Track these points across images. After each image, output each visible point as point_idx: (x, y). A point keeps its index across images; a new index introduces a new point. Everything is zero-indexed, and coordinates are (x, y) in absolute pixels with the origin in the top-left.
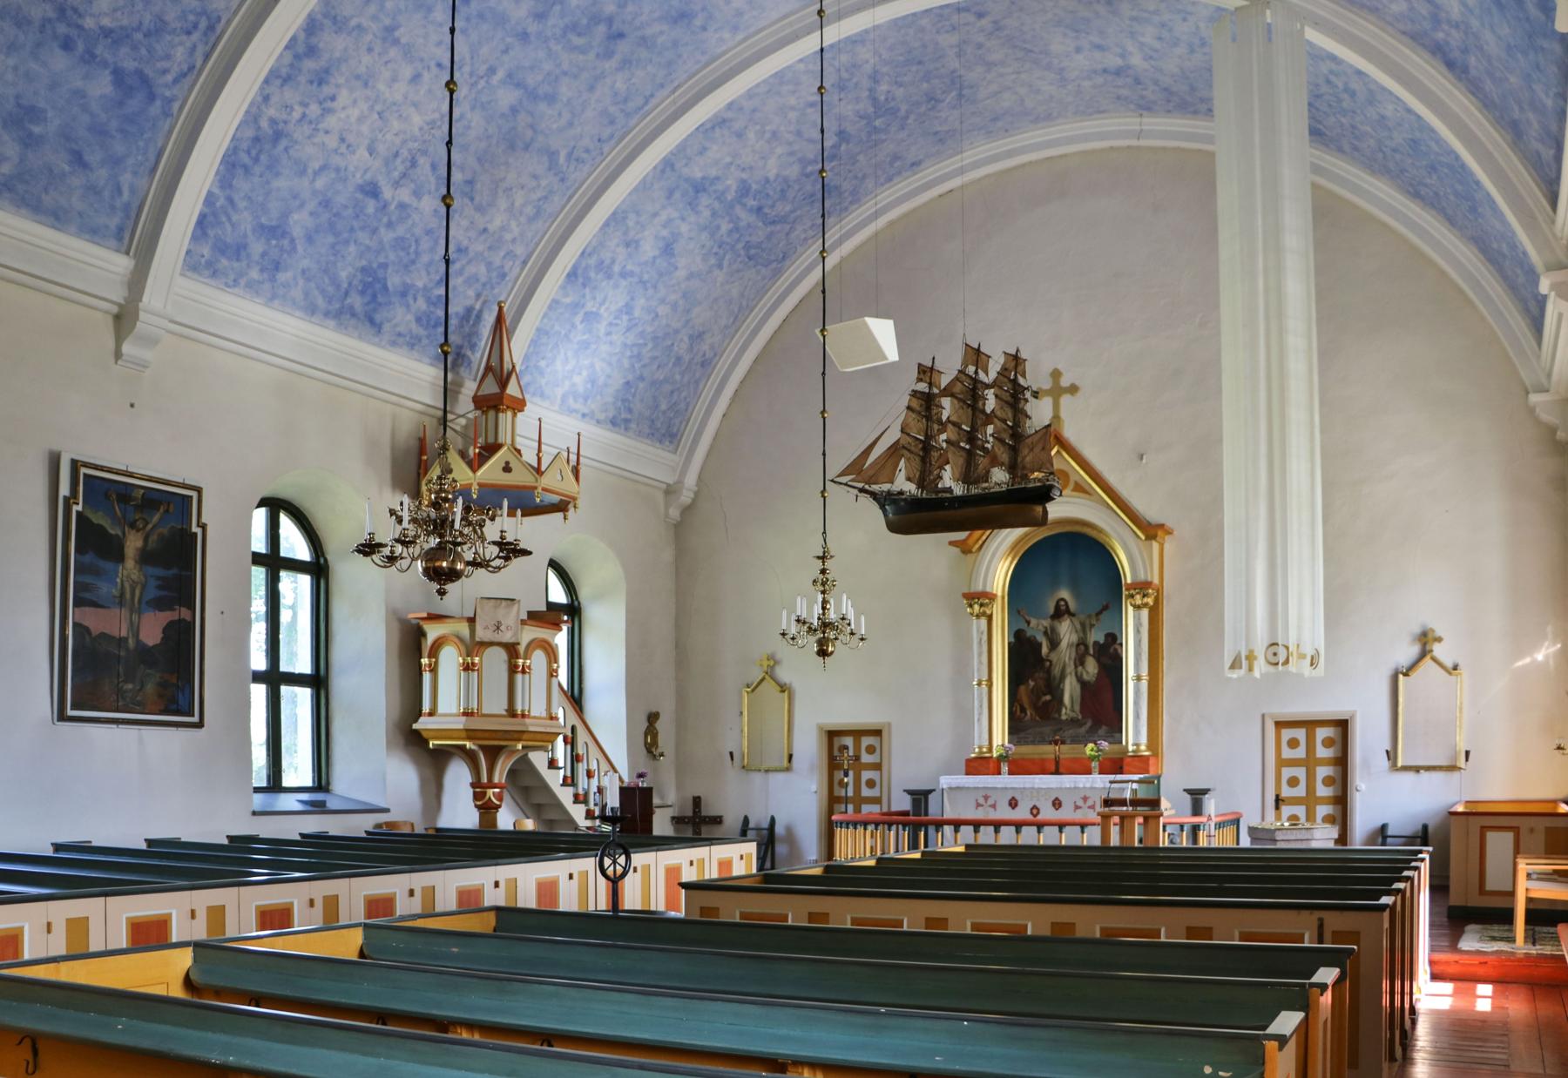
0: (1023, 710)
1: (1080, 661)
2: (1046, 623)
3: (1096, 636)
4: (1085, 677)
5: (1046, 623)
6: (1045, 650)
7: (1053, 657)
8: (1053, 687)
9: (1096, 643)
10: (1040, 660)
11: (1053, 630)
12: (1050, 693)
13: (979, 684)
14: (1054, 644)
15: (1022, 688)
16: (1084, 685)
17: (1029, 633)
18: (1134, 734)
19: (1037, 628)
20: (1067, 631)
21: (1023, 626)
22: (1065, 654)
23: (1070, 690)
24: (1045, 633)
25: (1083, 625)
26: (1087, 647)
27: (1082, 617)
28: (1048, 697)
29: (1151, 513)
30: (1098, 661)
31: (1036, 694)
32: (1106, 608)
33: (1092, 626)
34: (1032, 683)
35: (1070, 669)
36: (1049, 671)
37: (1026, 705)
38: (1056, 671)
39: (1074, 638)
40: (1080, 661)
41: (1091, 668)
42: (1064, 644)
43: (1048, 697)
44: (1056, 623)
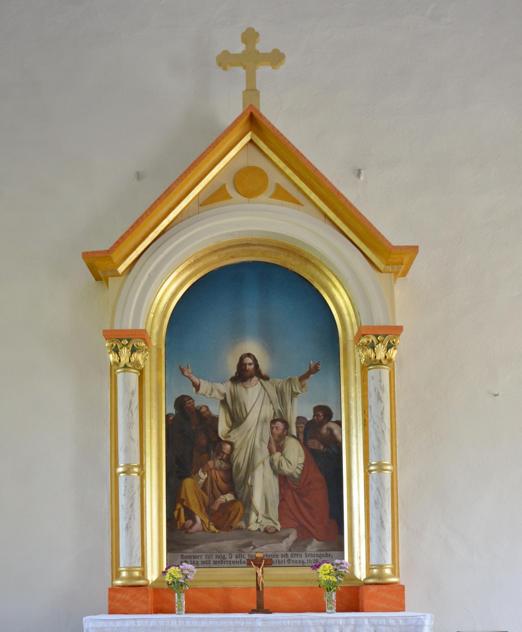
0: (190, 515)
1: (278, 445)
2: (226, 388)
3: (301, 409)
4: (286, 469)
5: (226, 388)
6: (223, 428)
7: (236, 437)
8: (235, 482)
9: (300, 419)
10: (216, 442)
11: (235, 398)
12: (231, 489)
13: (128, 471)
14: (237, 420)
15: (188, 482)
16: (284, 479)
17: (198, 402)
18: (358, 559)
19: (209, 396)
20: (255, 399)
21: (190, 391)
22: (250, 438)
23: (263, 488)
24: (224, 402)
25: (281, 393)
26: (287, 425)
27: (279, 381)
28: (229, 497)
29: (395, 239)
30: (305, 445)
31: (210, 490)
32: (314, 370)
33: (294, 394)
34: (203, 476)
35: (262, 455)
36: (229, 459)
37: (195, 507)
38: (241, 459)
39: (268, 412)
40: (278, 445)
41: (294, 456)
42: (252, 419)
43: (229, 497)
44: (240, 388)
